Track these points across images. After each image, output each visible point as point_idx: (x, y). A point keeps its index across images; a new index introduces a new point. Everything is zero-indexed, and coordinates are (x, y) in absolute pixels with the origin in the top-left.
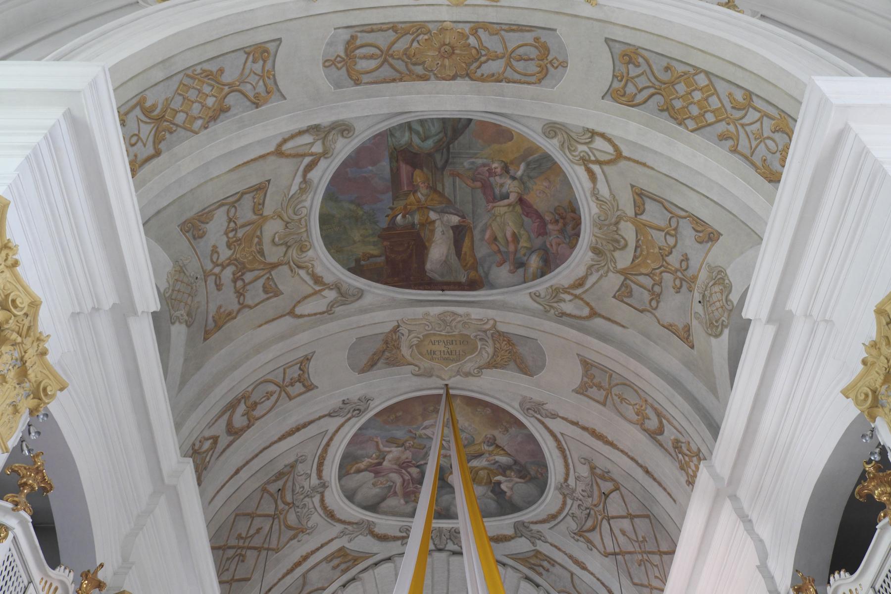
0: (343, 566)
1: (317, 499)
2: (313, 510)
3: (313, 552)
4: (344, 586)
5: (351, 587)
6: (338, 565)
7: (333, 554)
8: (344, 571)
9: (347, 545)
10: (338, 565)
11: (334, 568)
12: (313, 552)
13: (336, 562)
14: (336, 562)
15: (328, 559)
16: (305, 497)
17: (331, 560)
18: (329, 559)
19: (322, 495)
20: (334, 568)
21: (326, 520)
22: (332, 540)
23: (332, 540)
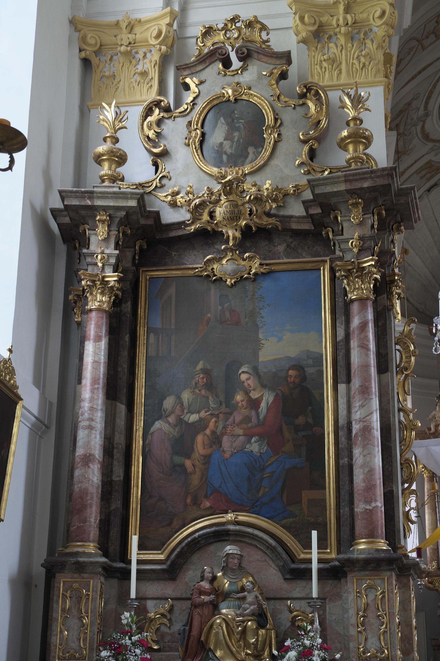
0: (428, 176)
1: (419, 128)
2: (415, 135)
3: (408, 168)
4: (429, 190)
5: (434, 192)
6: (425, 175)
7: (422, 167)
8: (429, 179)
9: (434, 159)
10: (425, 175)
11: (422, 178)
12: (408, 168)
13: (423, 173)
14: (423, 173)
15: (417, 172)
16: (412, 126)
17: (420, 172)
18: (419, 171)
19: (424, 122)
20: (422, 178)
21: (422, 142)
22: (423, 156)
23: (423, 156)
